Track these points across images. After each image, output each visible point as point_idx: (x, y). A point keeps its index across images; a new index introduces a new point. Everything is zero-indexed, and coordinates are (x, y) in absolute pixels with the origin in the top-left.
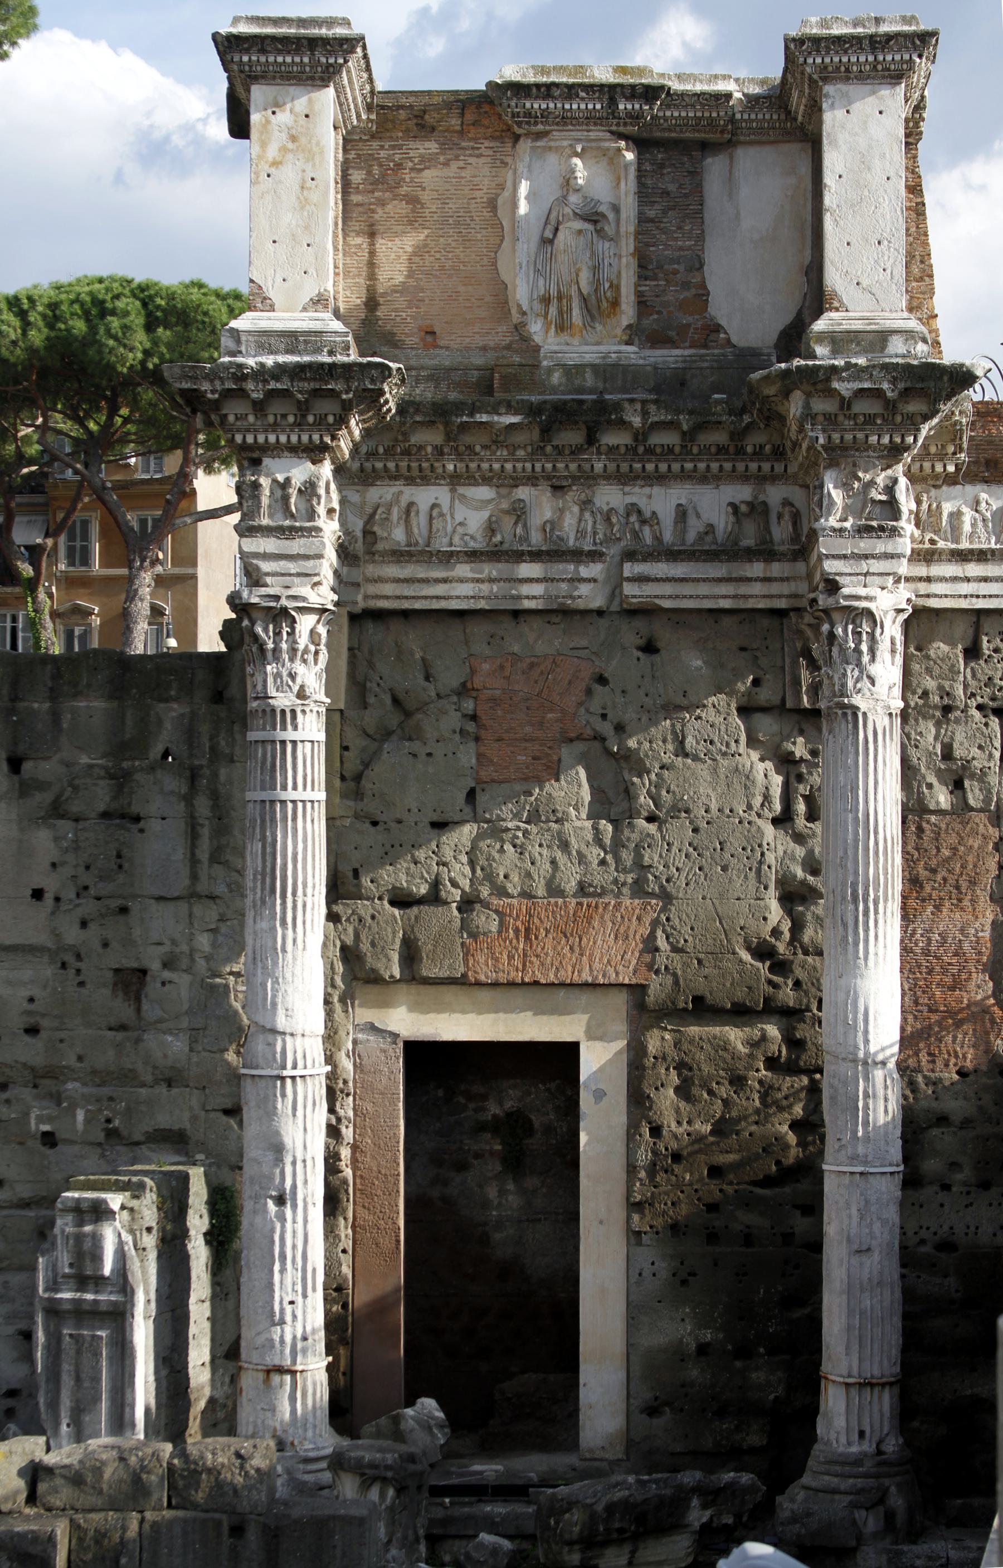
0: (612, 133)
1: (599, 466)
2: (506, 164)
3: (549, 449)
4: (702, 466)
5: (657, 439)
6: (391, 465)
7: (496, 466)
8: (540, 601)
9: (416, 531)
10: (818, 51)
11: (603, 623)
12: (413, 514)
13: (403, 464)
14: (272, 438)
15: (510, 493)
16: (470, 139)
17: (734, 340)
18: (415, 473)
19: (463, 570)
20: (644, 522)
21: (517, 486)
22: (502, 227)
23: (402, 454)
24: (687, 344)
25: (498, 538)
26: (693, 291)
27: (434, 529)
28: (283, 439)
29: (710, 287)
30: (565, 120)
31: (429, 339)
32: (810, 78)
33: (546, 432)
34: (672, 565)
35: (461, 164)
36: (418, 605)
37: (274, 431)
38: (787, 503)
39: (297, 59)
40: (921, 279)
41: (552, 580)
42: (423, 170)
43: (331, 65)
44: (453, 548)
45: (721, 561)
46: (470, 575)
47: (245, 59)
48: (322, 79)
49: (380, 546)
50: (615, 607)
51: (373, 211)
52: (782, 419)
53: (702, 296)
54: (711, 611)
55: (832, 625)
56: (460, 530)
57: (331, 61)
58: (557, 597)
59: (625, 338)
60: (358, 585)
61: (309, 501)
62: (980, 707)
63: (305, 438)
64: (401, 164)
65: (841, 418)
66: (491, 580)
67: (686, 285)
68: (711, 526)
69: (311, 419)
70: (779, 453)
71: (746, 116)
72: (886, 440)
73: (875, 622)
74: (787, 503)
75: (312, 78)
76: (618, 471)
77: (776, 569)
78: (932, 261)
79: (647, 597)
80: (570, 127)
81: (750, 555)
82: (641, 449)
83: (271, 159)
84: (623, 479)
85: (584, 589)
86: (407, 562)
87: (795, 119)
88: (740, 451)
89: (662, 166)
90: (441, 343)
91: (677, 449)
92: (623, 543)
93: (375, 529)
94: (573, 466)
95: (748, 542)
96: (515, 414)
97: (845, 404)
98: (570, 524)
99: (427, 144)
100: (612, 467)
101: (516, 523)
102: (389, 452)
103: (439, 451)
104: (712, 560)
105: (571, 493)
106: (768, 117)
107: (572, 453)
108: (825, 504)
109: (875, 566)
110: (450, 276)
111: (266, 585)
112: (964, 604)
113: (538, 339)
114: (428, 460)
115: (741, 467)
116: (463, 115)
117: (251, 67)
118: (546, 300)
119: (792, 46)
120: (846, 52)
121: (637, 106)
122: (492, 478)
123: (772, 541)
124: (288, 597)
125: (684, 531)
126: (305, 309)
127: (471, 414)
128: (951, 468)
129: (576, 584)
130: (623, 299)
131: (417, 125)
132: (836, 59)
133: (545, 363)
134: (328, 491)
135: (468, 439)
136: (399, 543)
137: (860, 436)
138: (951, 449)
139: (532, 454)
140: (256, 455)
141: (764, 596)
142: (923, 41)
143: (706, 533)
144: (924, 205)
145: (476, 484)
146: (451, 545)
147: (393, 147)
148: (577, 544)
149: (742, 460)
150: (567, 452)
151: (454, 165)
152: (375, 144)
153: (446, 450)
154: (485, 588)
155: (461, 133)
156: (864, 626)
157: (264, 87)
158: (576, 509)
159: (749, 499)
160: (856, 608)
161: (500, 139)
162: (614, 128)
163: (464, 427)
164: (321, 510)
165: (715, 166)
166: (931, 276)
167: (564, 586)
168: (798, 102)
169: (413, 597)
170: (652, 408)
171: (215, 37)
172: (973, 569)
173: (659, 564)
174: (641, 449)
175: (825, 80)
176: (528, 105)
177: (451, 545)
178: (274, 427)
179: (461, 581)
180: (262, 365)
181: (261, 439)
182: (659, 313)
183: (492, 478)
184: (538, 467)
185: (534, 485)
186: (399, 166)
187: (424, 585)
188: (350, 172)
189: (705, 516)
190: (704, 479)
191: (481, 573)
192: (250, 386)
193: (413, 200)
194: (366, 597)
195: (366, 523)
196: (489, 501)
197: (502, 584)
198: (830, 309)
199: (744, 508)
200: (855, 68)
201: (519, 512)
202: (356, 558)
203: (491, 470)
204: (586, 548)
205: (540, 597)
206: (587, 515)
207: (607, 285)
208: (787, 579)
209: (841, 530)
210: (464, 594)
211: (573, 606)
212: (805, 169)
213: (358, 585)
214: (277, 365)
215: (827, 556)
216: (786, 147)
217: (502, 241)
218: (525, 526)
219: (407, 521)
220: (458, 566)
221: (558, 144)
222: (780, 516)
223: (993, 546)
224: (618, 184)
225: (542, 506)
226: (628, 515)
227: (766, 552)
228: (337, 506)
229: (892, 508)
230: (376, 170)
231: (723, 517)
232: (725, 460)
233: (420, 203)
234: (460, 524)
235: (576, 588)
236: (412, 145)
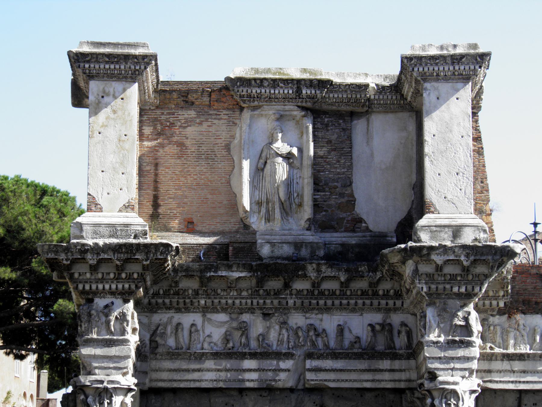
0: (298, 107)
1: (291, 302)
2: (235, 124)
3: (261, 292)
4: (352, 302)
5: (327, 286)
6: (167, 301)
7: (230, 301)
8: (256, 383)
9: (181, 340)
10: (421, 64)
11: (294, 396)
12: (179, 330)
13: (175, 300)
14: (100, 286)
15: (238, 318)
16: (215, 110)
17: (371, 227)
18: (181, 305)
19: (209, 364)
20: (318, 335)
21: (242, 313)
22: (234, 161)
23: (174, 294)
24: (343, 230)
25: (230, 345)
26: (346, 198)
27: (193, 339)
28: (107, 287)
29: (356, 196)
30: (270, 99)
31: (190, 226)
32: (416, 79)
33: (260, 283)
34: (335, 361)
35: (209, 124)
36: (182, 385)
37: (102, 282)
38: (403, 324)
39: (117, 67)
40: (482, 192)
41: (263, 370)
42: (187, 127)
43: (137, 70)
44: (204, 351)
45: (364, 359)
46: (214, 367)
47: (87, 66)
48: (131, 78)
49: (160, 350)
50: (300, 387)
51: (157, 151)
52: (401, 276)
53: (352, 202)
54: (358, 389)
55: (433, 399)
56: (208, 339)
57: (138, 68)
58: (266, 380)
59: (307, 226)
60: (146, 373)
61: (122, 324)
63: (120, 286)
64: (173, 124)
65: (436, 276)
66: (227, 370)
67: (342, 195)
68: (358, 338)
69: (124, 275)
70: (398, 295)
71: (377, 97)
72: (463, 290)
73: (459, 398)
74: (403, 324)
75: (126, 78)
76: (302, 305)
77: (397, 364)
78: (488, 182)
79: (320, 380)
80: (274, 103)
81: (382, 356)
82: (316, 292)
83: (101, 124)
84: (304, 309)
85: (282, 376)
86: (176, 359)
87: (406, 99)
88: (375, 294)
89: (327, 125)
90: (198, 228)
91: (338, 292)
92: (305, 348)
93: (157, 339)
94: (276, 302)
95: (380, 347)
96: (241, 272)
97: (439, 269)
98: (274, 337)
99: (189, 112)
100: (298, 302)
101: (242, 335)
102: (166, 294)
103: (196, 293)
104: (359, 358)
105: (274, 318)
106: (390, 97)
108: (427, 327)
110: (203, 189)
111: (95, 374)
112: (511, 386)
113: (254, 226)
114: (189, 298)
115: (375, 302)
116: (210, 96)
117: (90, 71)
118: (259, 204)
119: (405, 61)
120: (437, 64)
121: (313, 92)
122: (227, 308)
123: (394, 348)
125: (342, 341)
126: (120, 211)
127: (216, 271)
128: (502, 304)
129: (277, 372)
130: (305, 203)
131: (183, 101)
132: (431, 69)
133: (259, 241)
134: (133, 318)
135: (213, 285)
136: (171, 347)
137: (448, 286)
138: (501, 293)
139: (252, 295)
140: (90, 297)
141: (391, 381)
142: (482, 59)
143: (355, 342)
144: (482, 148)
145: (218, 312)
146: (202, 349)
147: (169, 114)
148: (278, 348)
149: (377, 299)
150: (272, 293)
151: (205, 124)
152: (159, 112)
153: (200, 292)
154: (223, 375)
155: (210, 106)
156: (452, 400)
157: (97, 82)
158: (277, 327)
159: (381, 322)
160: (447, 389)
161: (233, 110)
162: (299, 104)
163: (210, 278)
164: (129, 329)
165: (359, 127)
166: (487, 191)
167: (270, 374)
168: (408, 90)
169: (180, 380)
170: (323, 268)
171: (69, 53)
172: (517, 365)
173: (327, 361)
174: (316, 292)
175: (425, 80)
176: (249, 91)
177: (202, 349)
178: (102, 280)
179: (208, 370)
180: (96, 244)
181: (94, 287)
182: (326, 211)
183: (227, 308)
184: (255, 301)
185: (253, 313)
186: (172, 124)
187: (186, 373)
188: (144, 128)
189: (354, 332)
190: (353, 310)
191: (220, 365)
192: (89, 256)
193: (181, 145)
194: (151, 380)
195: (152, 335)
196: (226, 322)
197: (233, 372)
198: (429, 212)
199: (378, 328)
200: (442, 74)
201: (244, 329)
202: (146, 357)
203: (227, 303)
204: (284, 351)
205: (256, 380)
206: (284, 331)
207: (295, 195)
208: (404, 370)
209: (437, 342)
210: (210, 378)
212: (412, 127)
214: (105, 245)
215: (429, 358)
216: (400, 115)
217: (233, 169)
218: (247, 337)
219: (176, 334)
220: (207, 361)
221: (266, 113)
222: (399, 332)
223: (528, 351)
224: (302, 136)
225: (257, 326)
226: (308, 331)
227: (392, 354)
228: (137, 326)
229: (467, 329)
230: (159, 127)
231: (365, 332)
232: (366, 299)
233: (185, 146)
234: (209, 336)
235: (278, 375)
236: (180, 112)
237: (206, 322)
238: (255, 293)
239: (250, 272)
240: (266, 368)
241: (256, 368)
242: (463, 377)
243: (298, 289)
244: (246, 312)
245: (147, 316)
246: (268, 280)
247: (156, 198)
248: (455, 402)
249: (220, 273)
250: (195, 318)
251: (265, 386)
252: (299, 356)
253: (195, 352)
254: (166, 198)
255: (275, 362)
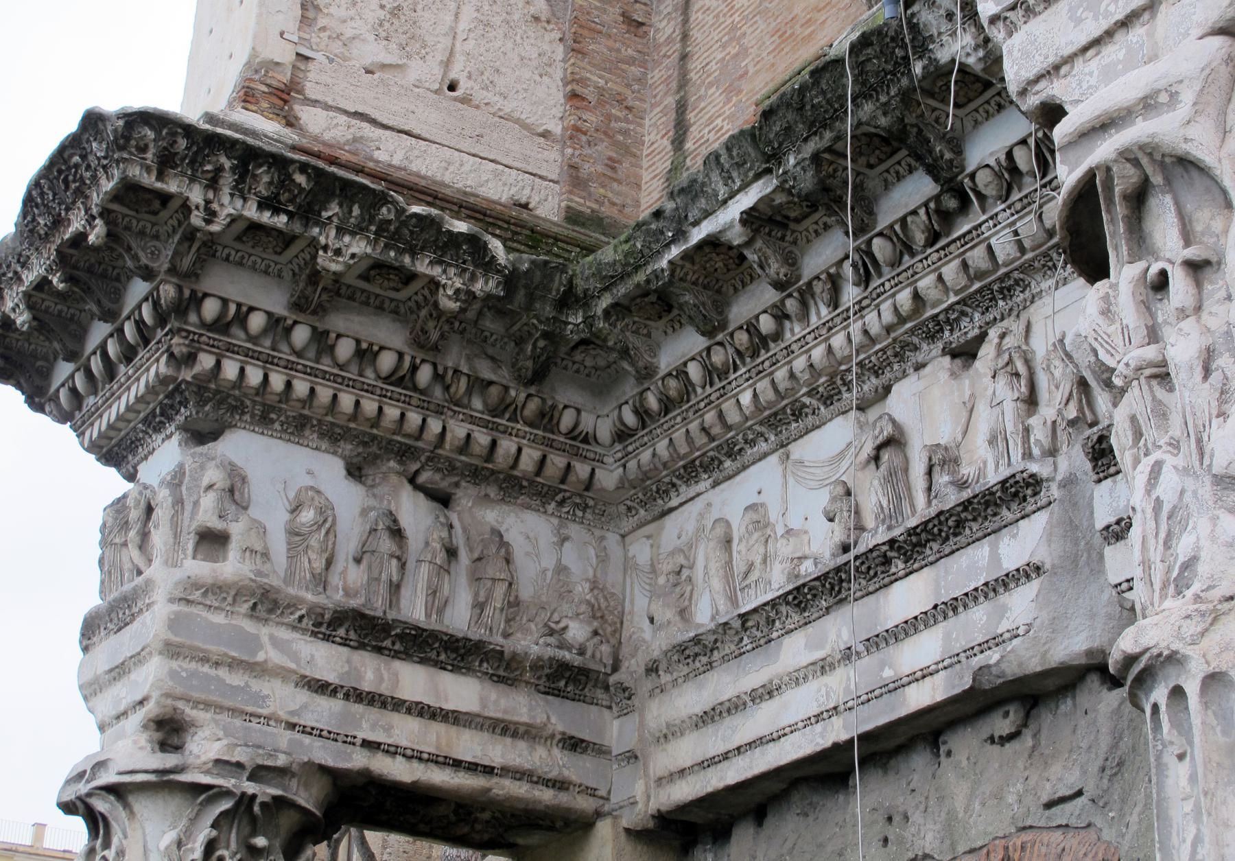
7: (818, 353)
13: (679, 435)
19: (795, 649)
21: (887, 390)
58: (970, 651)
85: (1021, 604)
86: (710, 666)
96: (744, 187)
107: (933, 238)
127: (680, 235)
129: (1004, 598)
169: (726, 756)
179: (797, 678)
211: (1012, 670)
220: (787, 640)
235: (1003, 611)
237: (791, 481)
238: (867, 270)
239: (768, 171)
240: (958, 593)
241: (928, 607)
243: (992, 163)
244: (898, 379)
245: (648, 537)
246: (887, 186)
247: (682, 108)
249: (697, 235)
250: (761, 480)
251: (967, 683)
252: (1069, 483)
253: (744, 617)
254: (702, 92)
255: (986, 549)
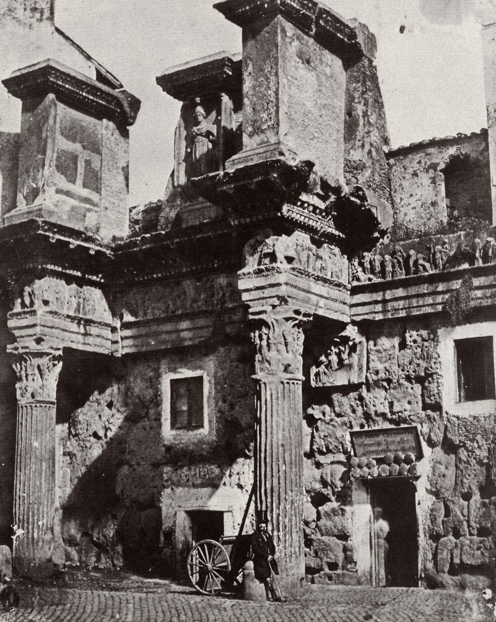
62: (408, 378)
109: (267, 292)
124: (23, 348)
213: (116, 342)
242: (274, 307)
248: (267, 332)
